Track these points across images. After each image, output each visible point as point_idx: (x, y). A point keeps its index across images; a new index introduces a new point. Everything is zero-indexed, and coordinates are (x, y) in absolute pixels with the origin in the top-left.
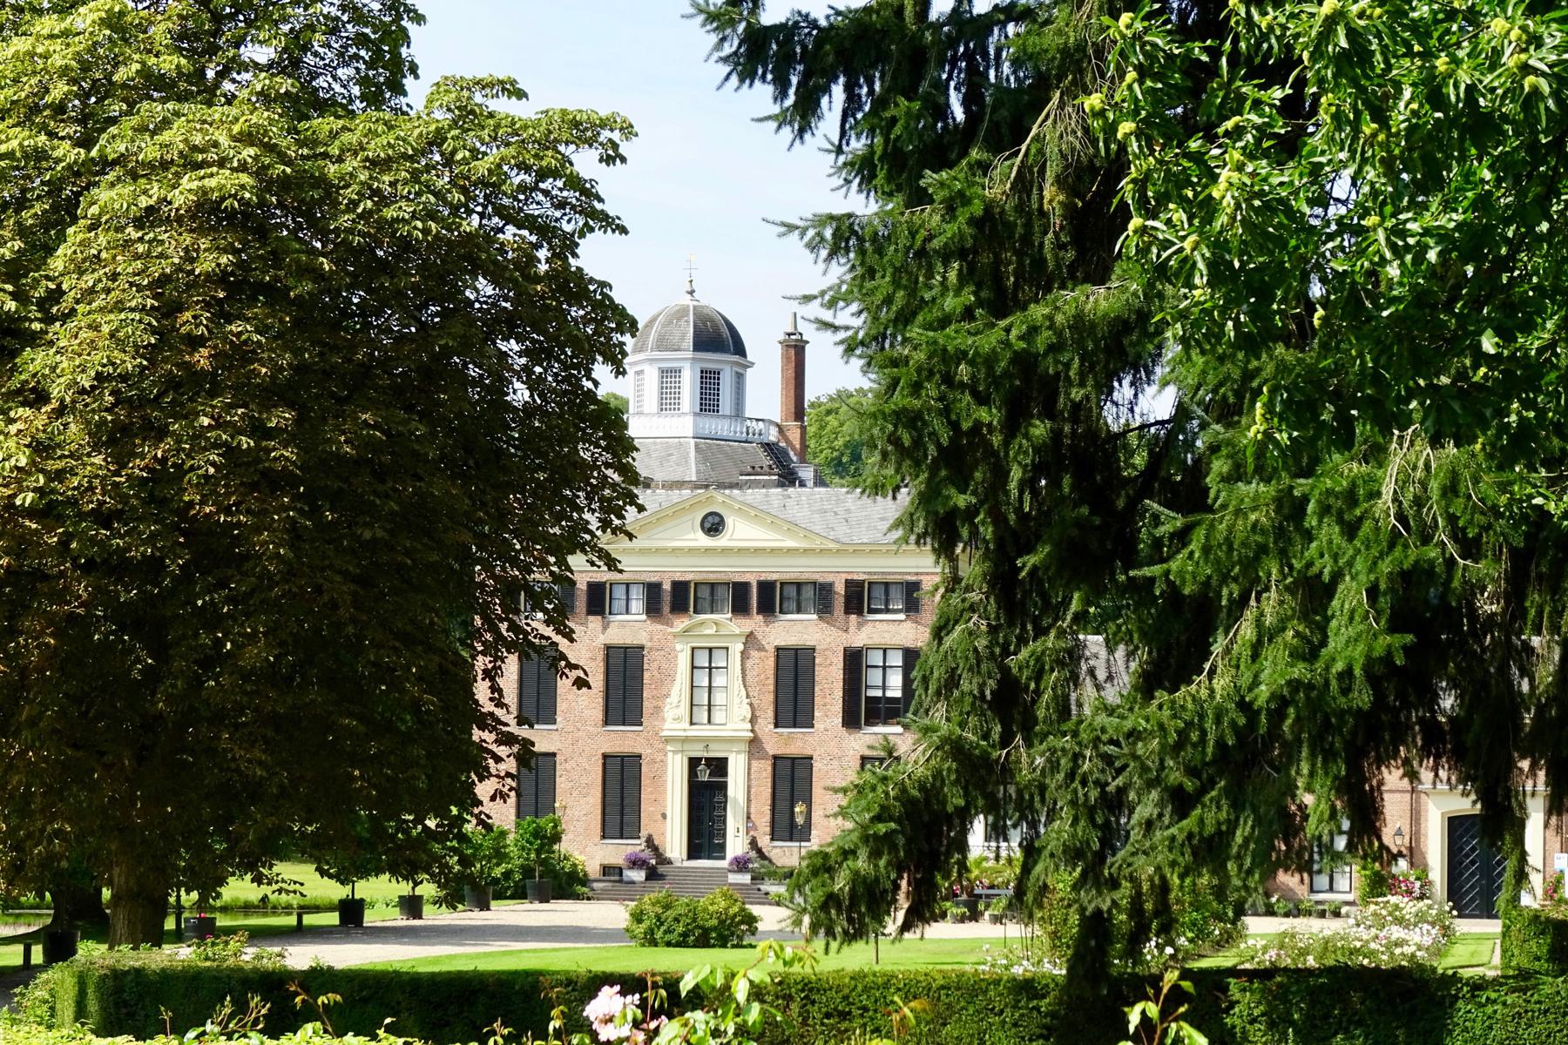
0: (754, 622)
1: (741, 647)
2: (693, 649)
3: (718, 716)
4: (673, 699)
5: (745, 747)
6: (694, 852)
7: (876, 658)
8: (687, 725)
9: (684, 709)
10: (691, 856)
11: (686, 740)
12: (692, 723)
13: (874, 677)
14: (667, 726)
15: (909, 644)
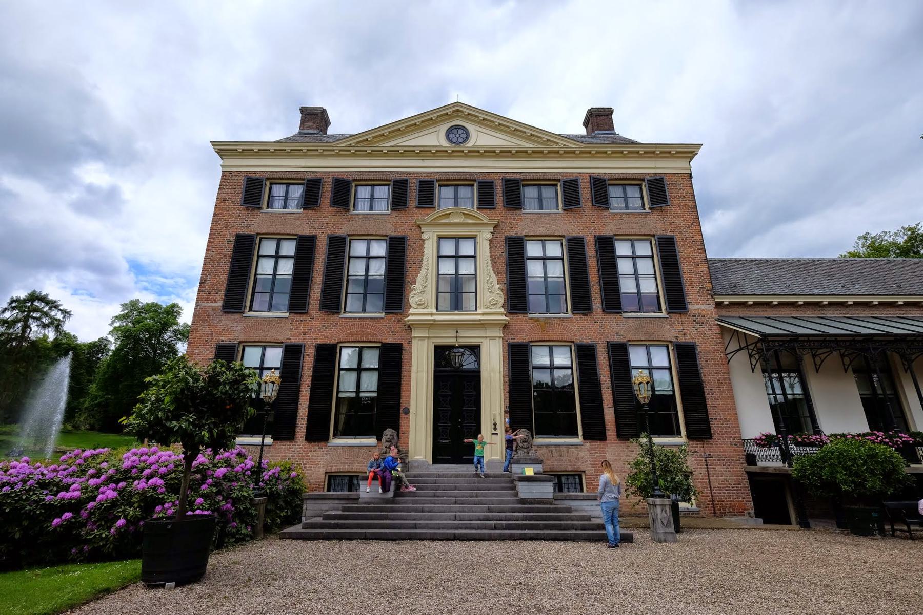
0: (500, 213)
1: (489, 236)
2: (440, 238)
3: (468, 301)
4: (418, 286)
5: (498, 333)
6: (441, 454)
7: (622, 248)
8: (434, 311)
9: (430, 296)
10: (435, 461)
11: (432, 325)
12: (437, 309)
13: (624, 267)
14: (411, 311)
15: (659, 232)
